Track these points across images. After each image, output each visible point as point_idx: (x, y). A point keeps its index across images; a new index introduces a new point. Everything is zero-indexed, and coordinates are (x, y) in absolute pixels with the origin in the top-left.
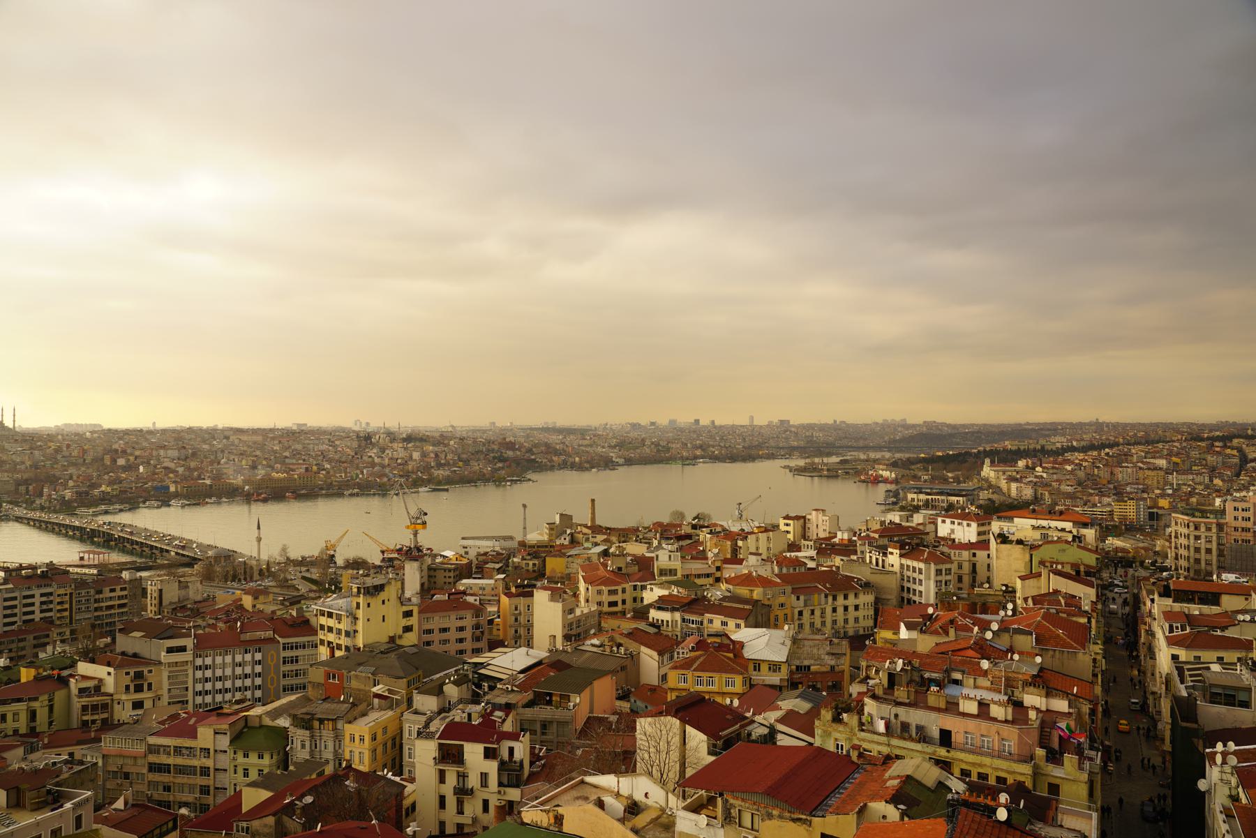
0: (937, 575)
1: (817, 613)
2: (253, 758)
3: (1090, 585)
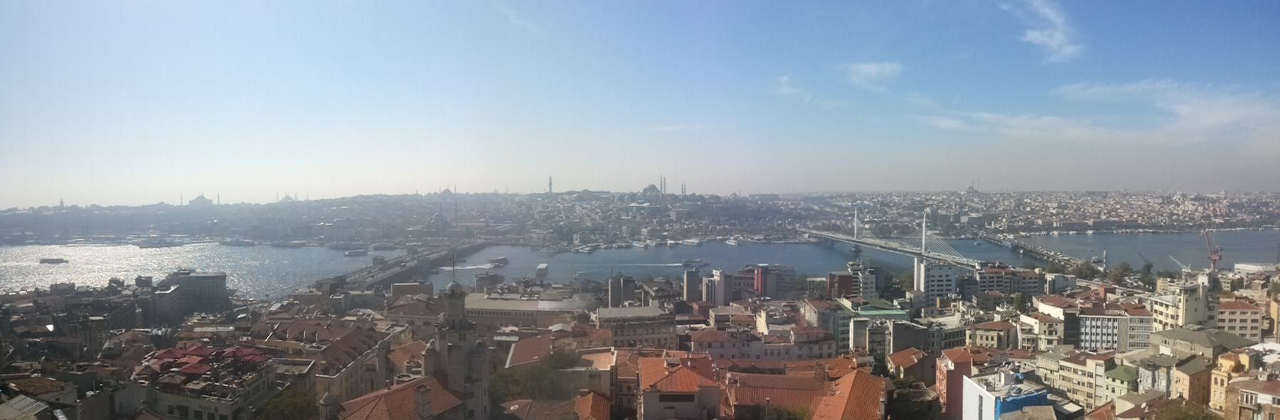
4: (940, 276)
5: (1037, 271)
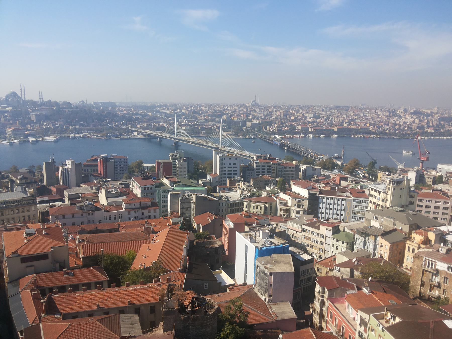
2: (340, 242)
4: (230, 164)
5: (294, 162)
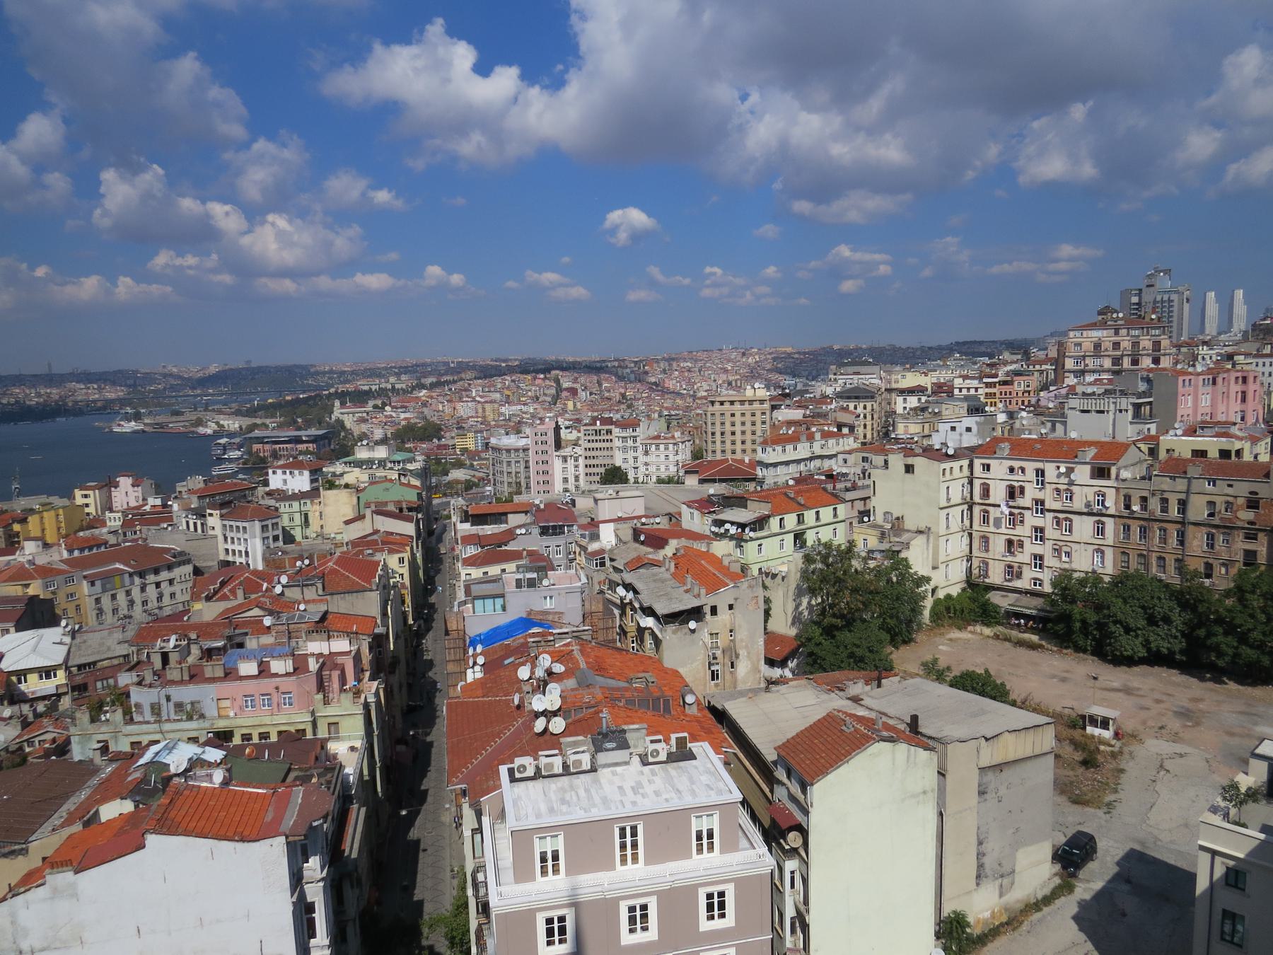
0: (263, 531)
1: (121, 597)
3: (409, 519)
